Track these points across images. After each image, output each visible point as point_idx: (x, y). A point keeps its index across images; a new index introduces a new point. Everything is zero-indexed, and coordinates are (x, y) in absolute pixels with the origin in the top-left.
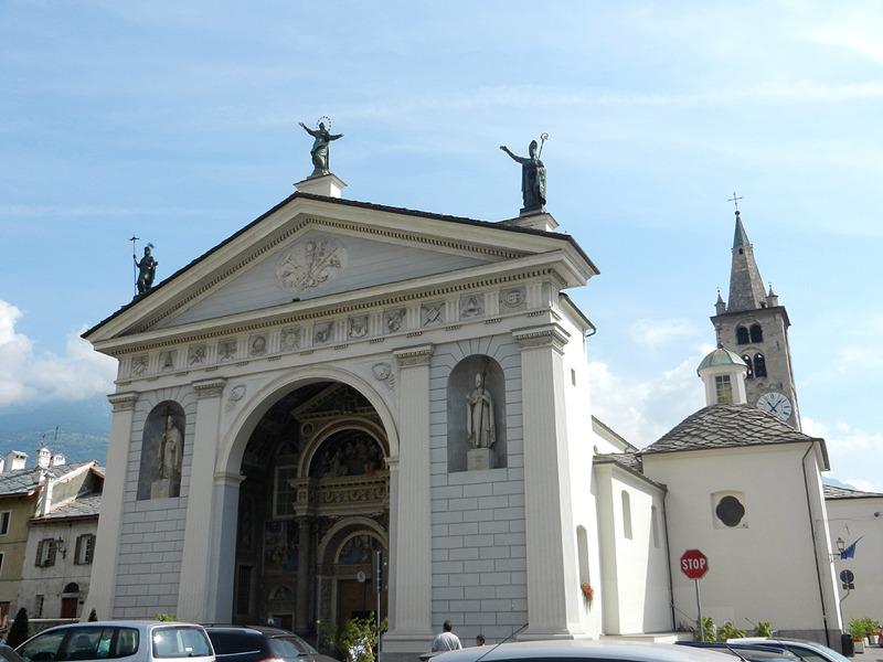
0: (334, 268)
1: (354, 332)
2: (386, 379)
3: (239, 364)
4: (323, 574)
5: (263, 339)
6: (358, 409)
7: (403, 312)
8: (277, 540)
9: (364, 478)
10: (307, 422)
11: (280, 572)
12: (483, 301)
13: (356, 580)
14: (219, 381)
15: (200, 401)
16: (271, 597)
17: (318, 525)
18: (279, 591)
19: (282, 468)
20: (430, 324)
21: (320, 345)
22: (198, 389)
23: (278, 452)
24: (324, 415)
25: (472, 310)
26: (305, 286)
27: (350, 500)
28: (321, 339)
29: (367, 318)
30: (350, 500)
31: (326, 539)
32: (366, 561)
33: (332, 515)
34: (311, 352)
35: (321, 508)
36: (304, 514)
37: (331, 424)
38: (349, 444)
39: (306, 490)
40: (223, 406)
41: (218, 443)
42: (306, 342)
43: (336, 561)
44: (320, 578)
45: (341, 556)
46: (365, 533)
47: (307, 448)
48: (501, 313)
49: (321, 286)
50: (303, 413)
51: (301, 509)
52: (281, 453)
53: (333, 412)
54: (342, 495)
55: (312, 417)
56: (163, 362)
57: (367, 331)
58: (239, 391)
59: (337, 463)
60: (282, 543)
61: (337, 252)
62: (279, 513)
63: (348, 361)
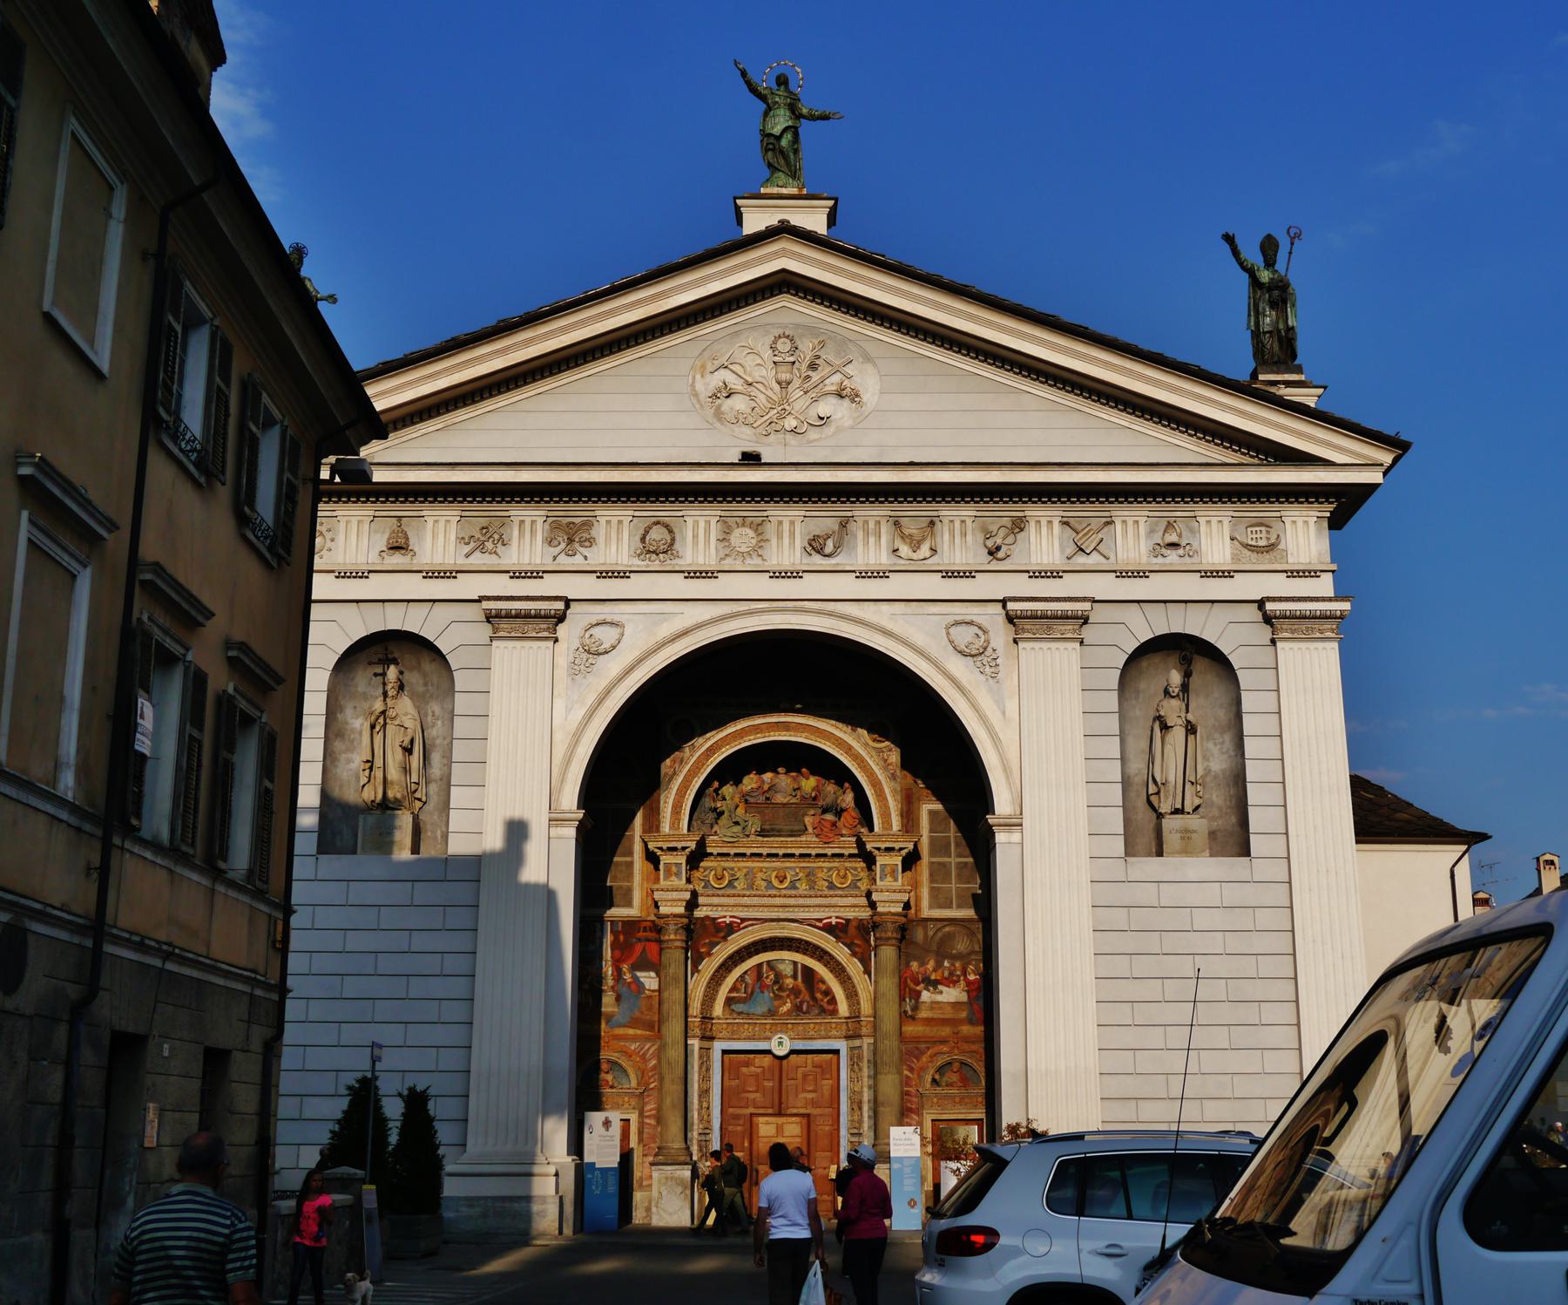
0: (846, 402)
1: (905, 550)
2: (976, 654)
3: (604, 574)
5: (671, 531)
7: (1019, 525)
9: (795, 845)
12: (1194, 532)
14: (560, 605)
15: (495, 643)
20: (1081, 561)
21: (818, 561)
22: (490, 617)
25: (1174, 545)
26: (773, 428)
27: (770, 885)
28: (820, 551)
29: (932, 523)
30: (770, 885)
31: (709, 966)
32: (789, 1013)
33: (725, 916)
34: (795, 575)
39: (682, 860)
40: (562, 662)
42: (786, 553)
43: (718, 1009)
44: (695, 1043)
45: (729, 1001)
48: (1236, 558)
49: (813, 434)
54: (750, 875)
56: (381, 542)
57: (934, 551)
58: (606, 635)
61: (849, 370)
63: (884, 607)
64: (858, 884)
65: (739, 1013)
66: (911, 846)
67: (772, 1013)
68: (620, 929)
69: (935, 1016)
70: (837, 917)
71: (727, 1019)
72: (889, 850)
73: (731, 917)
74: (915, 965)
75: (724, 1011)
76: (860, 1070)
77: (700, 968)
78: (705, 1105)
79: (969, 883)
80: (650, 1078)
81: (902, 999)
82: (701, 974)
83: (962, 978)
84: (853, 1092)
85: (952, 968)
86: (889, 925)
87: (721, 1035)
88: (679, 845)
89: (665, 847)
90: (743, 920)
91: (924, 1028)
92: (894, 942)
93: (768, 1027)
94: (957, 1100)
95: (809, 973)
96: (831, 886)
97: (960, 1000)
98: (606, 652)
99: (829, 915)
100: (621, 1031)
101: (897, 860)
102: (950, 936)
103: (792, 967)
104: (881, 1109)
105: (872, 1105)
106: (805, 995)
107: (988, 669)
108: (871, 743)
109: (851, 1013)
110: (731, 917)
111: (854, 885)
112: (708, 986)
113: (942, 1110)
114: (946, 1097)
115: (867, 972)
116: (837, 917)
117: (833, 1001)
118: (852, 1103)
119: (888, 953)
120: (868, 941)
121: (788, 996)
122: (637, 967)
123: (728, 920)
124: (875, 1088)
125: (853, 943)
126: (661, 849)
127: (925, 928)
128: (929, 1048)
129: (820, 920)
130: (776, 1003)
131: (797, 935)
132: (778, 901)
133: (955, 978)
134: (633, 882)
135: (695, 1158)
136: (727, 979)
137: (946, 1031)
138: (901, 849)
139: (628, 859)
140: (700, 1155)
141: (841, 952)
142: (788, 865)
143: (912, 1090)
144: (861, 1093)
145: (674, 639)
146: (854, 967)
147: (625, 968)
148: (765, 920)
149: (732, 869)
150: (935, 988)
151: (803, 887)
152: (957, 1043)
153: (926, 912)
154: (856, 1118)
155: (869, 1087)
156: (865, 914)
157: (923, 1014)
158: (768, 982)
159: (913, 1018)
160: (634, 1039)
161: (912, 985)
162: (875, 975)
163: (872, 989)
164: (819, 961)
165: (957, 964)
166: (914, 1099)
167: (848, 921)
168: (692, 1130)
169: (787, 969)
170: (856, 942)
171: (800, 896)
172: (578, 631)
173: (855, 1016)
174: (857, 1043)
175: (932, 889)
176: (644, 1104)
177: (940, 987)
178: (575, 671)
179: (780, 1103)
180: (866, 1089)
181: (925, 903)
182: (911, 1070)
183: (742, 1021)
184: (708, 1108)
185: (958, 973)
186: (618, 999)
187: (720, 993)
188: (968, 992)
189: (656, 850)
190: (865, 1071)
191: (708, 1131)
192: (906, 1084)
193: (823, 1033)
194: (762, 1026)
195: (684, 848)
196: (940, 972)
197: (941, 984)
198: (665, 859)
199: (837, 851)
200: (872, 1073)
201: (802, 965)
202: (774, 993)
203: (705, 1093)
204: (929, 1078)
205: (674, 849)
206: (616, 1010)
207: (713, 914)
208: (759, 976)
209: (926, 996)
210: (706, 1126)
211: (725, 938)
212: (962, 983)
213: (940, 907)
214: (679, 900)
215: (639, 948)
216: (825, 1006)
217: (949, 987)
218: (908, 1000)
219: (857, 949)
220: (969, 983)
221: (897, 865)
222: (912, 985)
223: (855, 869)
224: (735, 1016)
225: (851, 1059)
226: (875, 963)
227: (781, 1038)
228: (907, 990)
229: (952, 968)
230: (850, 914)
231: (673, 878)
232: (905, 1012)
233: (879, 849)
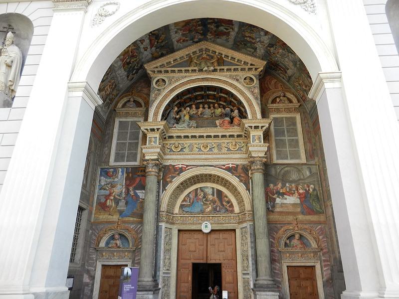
4: (167, 222)
6: (219, 68)
8: (113, 186)
9: (212, 132)
10: (160, 76)
11: (115, 218)
13: (201, 231)
16: (102, 244)
17: (166, 172)
18: (113, 238)
19: (124, 120)
23: (120, 105)
24: (180, 71)
31: (171, 188)
32: (210, 212)
33: (179, 164)
35: (168, 157)
36: (156, 157)
37: (185, 80)
38: (194, 106)
39: (158, 136)
41: (77, 49)
43: (177, 210)
44: (163, 225)
45: (182, 206)
46: (209, 185)
47: (160, 98)
50: (157, 67)
51: (151, 151)
52: (124, 106)
53: (190, 69)
54: (191, 147)
55: (167, 72)
59: (187, 117)
60: (120, 189)
62: (116, 161)
64: (242, 149)
65: (186, 212)
66: (267, 125)
67: (202, 212)
68: (130, 171)
69: (284, 210)
70: (232, 164)
71: (180, 214)
72: (256, 127)
73: (182, 165)
74: (271, 185)
75: (179, 211)
76: (247, 239)
77: (166, 188)
78: (167, 257)
79: (295, 148)
80: (139, 243)
81: (267, 202)
82: (167, 191)
83: (296, 192)
84: (243, 251)
85: (291, 187)
86: (258, 162)
87: (178, 222)
88: (155, 127)
89: (148, 129)
90: (187, 166)
91: (279, 216)
92: (261, 171)
93: (200, 218)
94: (300, 255)
95: (220, 193)
96: (229, 149)
97: (296, 203)
98: (110, 15)
99: (229, 163)
100: (126, 219)
101: (260, 133)
102: (288, 172)
103: (211, 190)
104: (259, 259)
105: (254, 257)
106: (218, 203)
107: (309, 9)
108: (245, 85)
109: (240, 211)
110: (182, 165)
111: (240, 149)
112: (171, 198)
113: (292, 260)
114: (293, 253)
115: (248, 189)
116: (232, 164)
117: (232, 206)
118: (243, 257)
119: (258, 178)
120: (248, 175)
121: (210, 203)
122: (136, 188)
123: (180, 166)
124: (255, 249)
125: (240, 175)
126: (147, 129)
127: (275, 168)
128: (282, 227)
129: (224, 165)
130: (204, 207)
131: (213, 173)
132: (204, 157)
133: (292, 192)
134: (137, 151)
135: (160, 286)
136: (181, 196)
137: (290, 218)
138: (262, 127)
139: (136, 141)
140: (163, 285)
141: (234, 180)
142: (209, 141)
143: (275, 250)
144: (247, 251)
145: (144, 7)
146: (241, 188)
147: (131, 189)
148: (198, 166)
149: (183, 144)
150: (283, 196)
151: (216, 151)
152: (297, 224)
153: (275, 161)
154: (246, 265)
155: (252, 248)
156: (245, 162)
157: (278, 209)
158: (201, 197)
159: (273, 212)
160: (133, 223)
161: (271, 195)
162: (252, 190)
163: (251, 197)
164: (224, 186)
165: (293, 185)
166: (276, 254)
167: (237, 165)
168: (159, 271)
169: (210, 191)
170: (242, 175)
171: (214, 154)
172: (99, 7)
173: (242, 211)
174: (244, 225)
175: (277, 151)
176: (135, 256)
177: (285, 196)
178: (94, 23)
179: (207, 257)
180: (250, 249)
181: (275, 157)
182: (274, 238)
183: (187, 215)
184: (170, 259)
185: (294, 189)
186: (127, 203)
187: (178, 202)
188: (300, 198)
189: (145, 131)
190: (249, 240)
191: (169, 272)
192: (272, 246)
193: (227, 221)
194: (197, 218)
195: (158, 129)
196: (284, 188)
197: (286, 195)
198: (150, 135)
199: (231, 134)
200: (253, 240)
201: (217, 189)
202: (203, 202)
203: (168, 251)
204: (283, 243)
205: (153, 130)
206: (125, 208)
207: (173, 164)
208: (196, 195)
209: (278, 200)
210: (168, 268)
211: (179, 174)
212: (296, 194)
213: (282, 159)
214: (154, 153)
215: (138, 180)
216: (228, 208)
217: (289, 196)
218: (269, 203)
219: (242, 179)
220: (300, 194)
221: (260, 135)
222: (271, 195)
223: (240, 143)
224: (185, 213)
225: (242, 234)
226: (252, 184)
227: (206, 224)
228: (269, 198)
229: (291, 187)
230: (238, 163)
231: (153, 143)
232: (268, 209)
233: (251, 127)
